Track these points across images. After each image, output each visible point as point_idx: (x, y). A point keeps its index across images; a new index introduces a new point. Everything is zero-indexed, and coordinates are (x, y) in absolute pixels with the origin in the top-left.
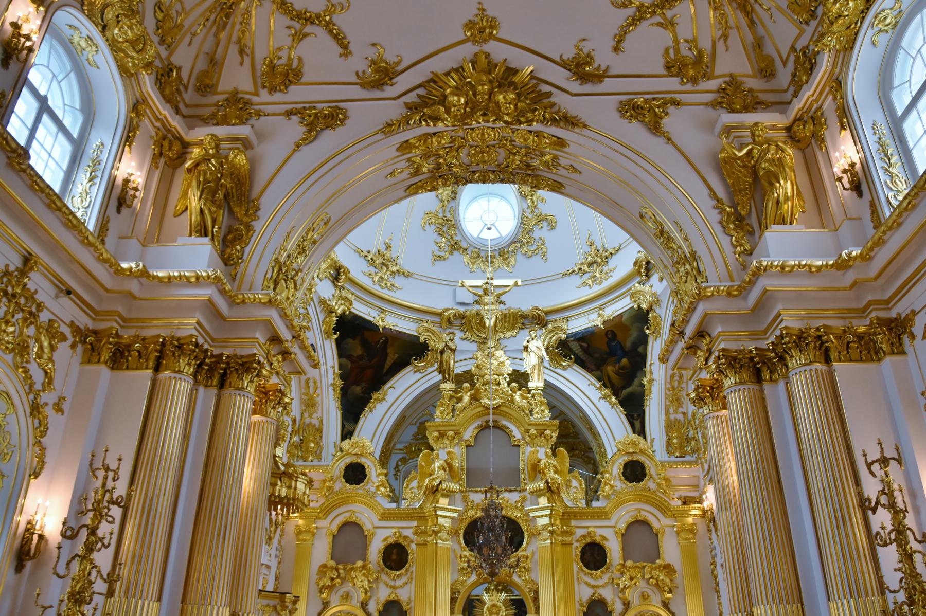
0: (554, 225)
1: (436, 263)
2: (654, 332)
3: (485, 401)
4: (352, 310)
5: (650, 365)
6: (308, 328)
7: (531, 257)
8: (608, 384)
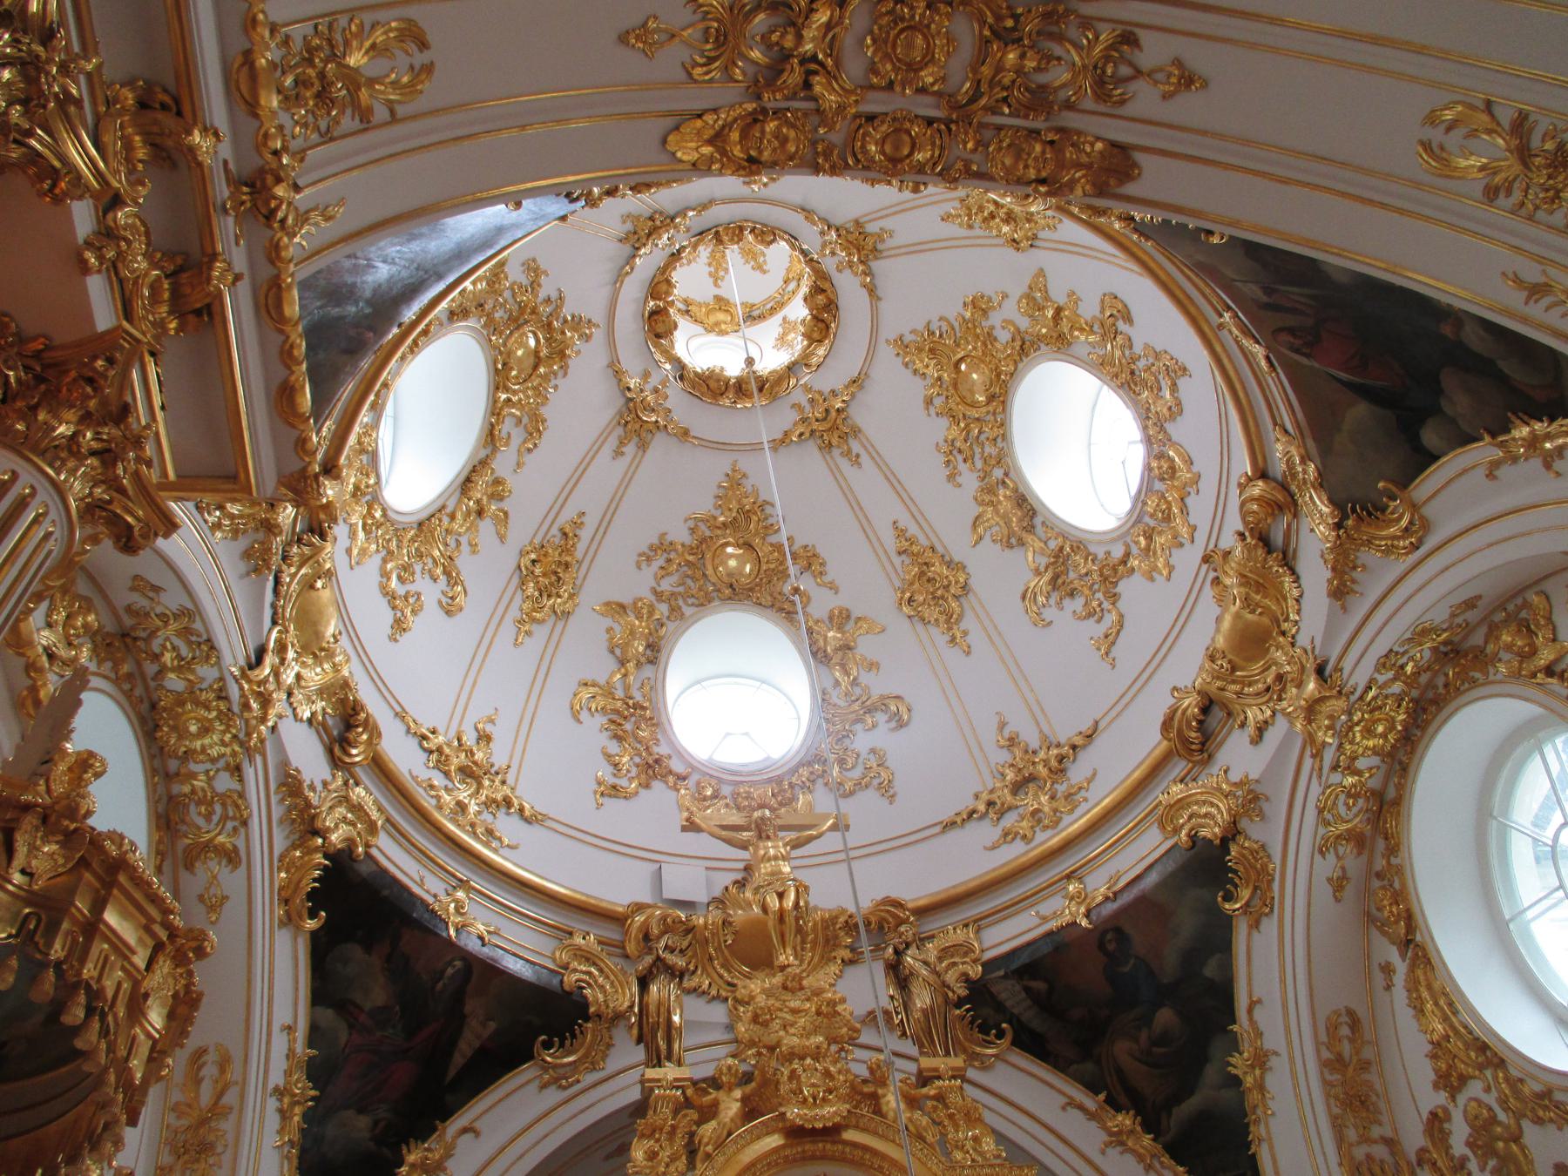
0: (906, 717)
1: (606, 800)
2: (1247, 904)
3: (794, 1112)
4: (374, 852)
5: (1250, 1011)
6: (232, 857)
7: (852, 793)
8: (1123, 1099)
